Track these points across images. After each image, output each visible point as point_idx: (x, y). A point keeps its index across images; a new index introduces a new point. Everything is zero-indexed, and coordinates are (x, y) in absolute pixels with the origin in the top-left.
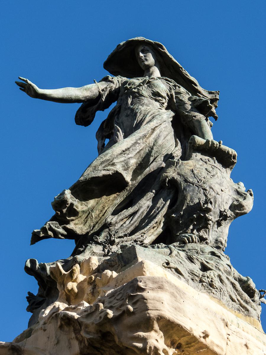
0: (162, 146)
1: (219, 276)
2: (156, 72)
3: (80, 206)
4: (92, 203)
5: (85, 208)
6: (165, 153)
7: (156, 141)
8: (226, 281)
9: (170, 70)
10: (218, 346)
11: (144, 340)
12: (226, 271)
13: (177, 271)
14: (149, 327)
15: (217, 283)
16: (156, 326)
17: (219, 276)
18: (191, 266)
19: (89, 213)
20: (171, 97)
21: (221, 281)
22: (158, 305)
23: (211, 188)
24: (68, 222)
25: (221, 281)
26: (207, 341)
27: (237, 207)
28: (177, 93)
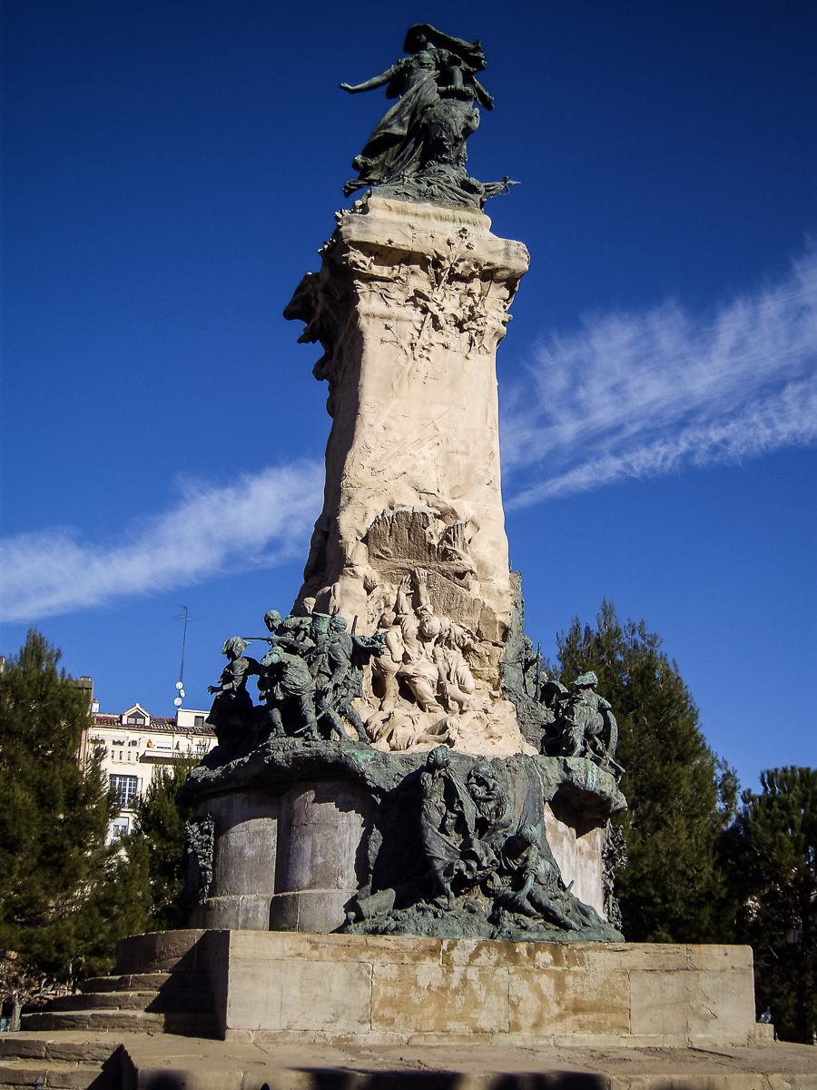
0: (424, 101)
1: (439, 187)
2: (431, 46)
3: (373, 162)
4: (382, 156)
5: (377, 162)
6: (425, 104)
7: (419, 98)
8: (445, 188)
9: (441, 42)
10: (403, 245)
11: (347, 258)
12: (445, 182)
13: (406, 194)
14: (348, 251)
15: (437, 192)
16: (351, 248)
17: (439, 187)
18: (419, 186)
19: (382, 163)
20: (436, 61)
21: (442, 189)
22: (348, 234)
23: (446, 123)
24: (369, 175)
25: (442, 189)
26: (393, 245)
27: (467, 131)
28: (441, 56)
